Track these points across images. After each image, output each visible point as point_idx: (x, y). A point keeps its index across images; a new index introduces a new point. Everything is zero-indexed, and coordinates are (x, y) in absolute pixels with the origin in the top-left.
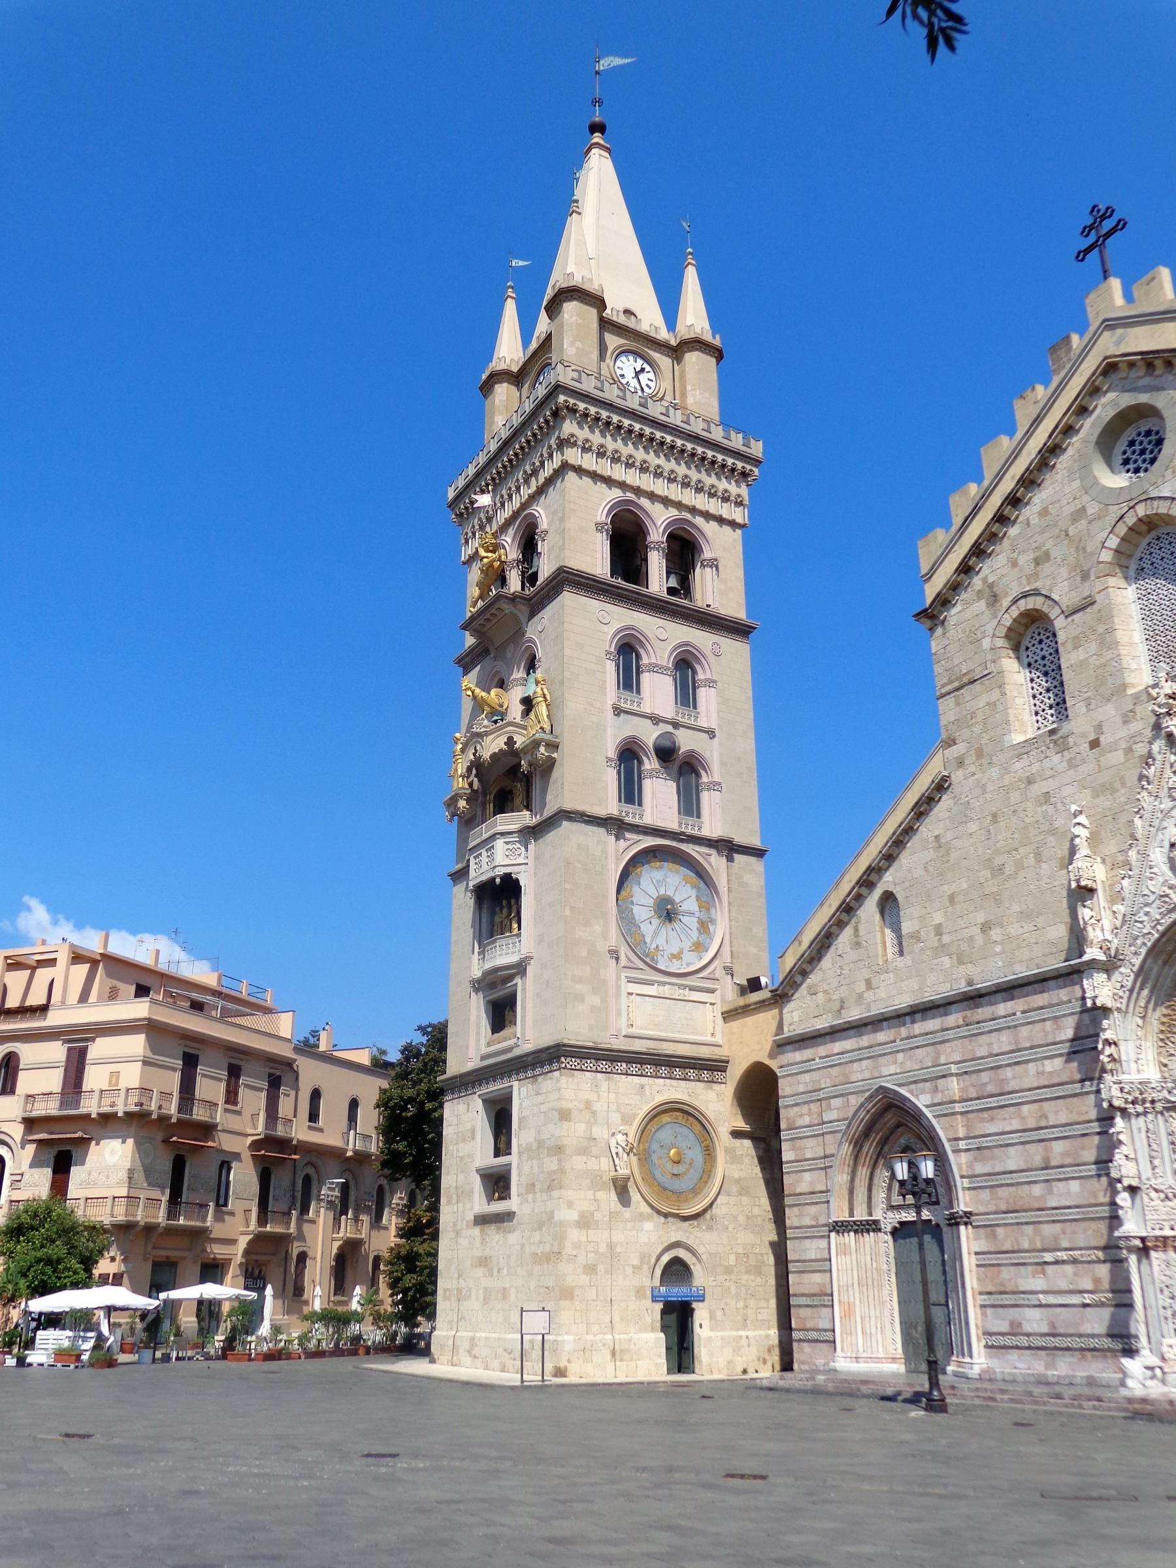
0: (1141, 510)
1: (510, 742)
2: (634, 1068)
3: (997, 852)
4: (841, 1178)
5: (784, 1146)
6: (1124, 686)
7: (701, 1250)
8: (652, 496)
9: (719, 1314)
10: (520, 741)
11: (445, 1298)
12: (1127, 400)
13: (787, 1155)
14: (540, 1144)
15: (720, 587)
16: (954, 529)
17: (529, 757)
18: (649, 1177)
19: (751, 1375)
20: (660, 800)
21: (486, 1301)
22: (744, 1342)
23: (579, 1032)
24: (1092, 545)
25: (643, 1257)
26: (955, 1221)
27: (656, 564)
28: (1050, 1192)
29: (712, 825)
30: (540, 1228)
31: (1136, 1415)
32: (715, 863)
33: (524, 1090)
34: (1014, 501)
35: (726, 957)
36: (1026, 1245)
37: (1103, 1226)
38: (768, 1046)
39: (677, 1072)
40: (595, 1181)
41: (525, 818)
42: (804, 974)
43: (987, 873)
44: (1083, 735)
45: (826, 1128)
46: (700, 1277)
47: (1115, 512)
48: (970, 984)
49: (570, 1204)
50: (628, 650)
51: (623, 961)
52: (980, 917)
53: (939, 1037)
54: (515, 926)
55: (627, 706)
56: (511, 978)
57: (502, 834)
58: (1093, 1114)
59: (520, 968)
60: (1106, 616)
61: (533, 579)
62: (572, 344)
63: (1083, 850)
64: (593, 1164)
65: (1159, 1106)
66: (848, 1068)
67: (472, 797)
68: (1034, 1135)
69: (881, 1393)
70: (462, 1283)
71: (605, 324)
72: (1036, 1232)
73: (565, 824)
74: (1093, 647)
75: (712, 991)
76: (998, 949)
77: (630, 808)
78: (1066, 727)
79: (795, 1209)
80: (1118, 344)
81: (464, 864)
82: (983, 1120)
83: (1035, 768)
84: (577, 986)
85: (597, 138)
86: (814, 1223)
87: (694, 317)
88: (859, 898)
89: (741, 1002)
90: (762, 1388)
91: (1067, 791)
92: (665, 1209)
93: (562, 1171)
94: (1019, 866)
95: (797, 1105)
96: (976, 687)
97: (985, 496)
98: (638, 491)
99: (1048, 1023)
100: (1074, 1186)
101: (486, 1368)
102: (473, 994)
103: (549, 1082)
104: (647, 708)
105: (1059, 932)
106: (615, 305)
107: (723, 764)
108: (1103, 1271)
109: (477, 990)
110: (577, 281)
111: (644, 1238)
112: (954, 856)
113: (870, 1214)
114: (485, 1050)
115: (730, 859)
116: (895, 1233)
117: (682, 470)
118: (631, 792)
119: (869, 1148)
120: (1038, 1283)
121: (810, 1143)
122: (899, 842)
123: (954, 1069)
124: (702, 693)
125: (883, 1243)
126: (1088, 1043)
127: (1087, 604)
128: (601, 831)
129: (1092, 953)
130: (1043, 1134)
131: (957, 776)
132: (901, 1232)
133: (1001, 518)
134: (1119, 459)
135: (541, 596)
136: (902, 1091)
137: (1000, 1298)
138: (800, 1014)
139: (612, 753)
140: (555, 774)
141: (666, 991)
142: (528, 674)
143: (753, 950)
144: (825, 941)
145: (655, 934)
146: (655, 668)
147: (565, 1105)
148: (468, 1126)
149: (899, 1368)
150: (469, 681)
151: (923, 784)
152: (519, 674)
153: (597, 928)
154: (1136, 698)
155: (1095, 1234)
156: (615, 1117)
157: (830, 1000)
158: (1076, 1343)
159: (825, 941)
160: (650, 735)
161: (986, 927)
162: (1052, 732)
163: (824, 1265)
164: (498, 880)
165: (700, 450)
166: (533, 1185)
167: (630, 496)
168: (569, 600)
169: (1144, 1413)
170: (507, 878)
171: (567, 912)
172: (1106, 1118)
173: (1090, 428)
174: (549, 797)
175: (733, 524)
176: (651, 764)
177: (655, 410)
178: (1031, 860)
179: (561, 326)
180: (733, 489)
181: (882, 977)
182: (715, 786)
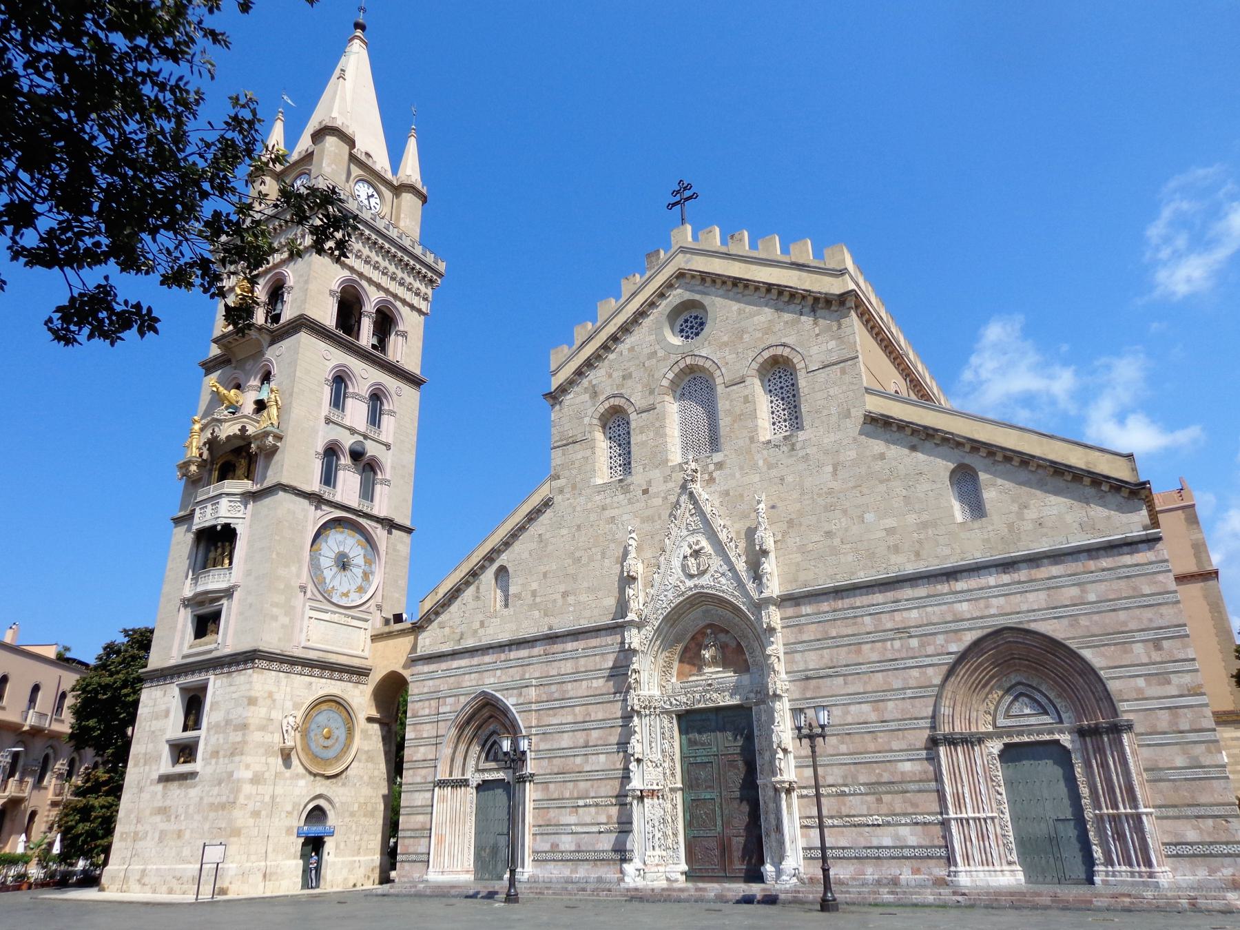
0: (688, 361)
1: (243, 429)
2: (307, 670)
4: (447, 751)
5: (408, 729)
6: (667, 460)
7: (336, 800)
8: (370, 281)
9: (342, 845)
10: (251, 430)
11: (122, 839)
12: (688, 296)
13: (410, 734)
14: (228, 722)
15: (406, 350)
16: (575, 347)
17: (258, 442)
18: (307, 748)
19: (359, 888)
20: (348, 487)
21: (161, 840)
22: (357, 864)
23: (270, 642)
24: (658, 375)
25: (295, 805)
26: (522, 780)
27: (367, 326)
28: (587, 761)
29: (380, 507)
30: (220, 784)
31: (632, 899)
32: (379, 533)
33: (219, 682)
34: (615, 338)
35: (378, 598)
36: (567, 795)
37: (617, 783)
38: (403, 661)
39: (336, 675)
40: (268, 752)
41: (248, 485)
42: (437, 614)
43: (570, 561)
44: (639, 485)
46: (332, 819)
47: (674, 358)
48: (550, 629)
49: (247, 767)
50: (340, 380)
51: (309, 595)
52: (562, 588)
53: (526, 661)
54: (227, 561)
55: (335, 418)
56: (221, 598)
57: (228, 494)
58: (619, 714)
59: (228, 593)
60: (662, 418)
61: (276, 318)
62: (329, 165)
63: (633, 554)
64: (268, 738)
65: (658, 711)
66: (461, 678)
67: (202, 464)
68: (581, 726)
69: (465, 892)
70: (140, 827)
71: (353, 158)
73: (281, 493)
74: (651, 435)
75: (366, 621)
76: (571, 609)
77: (326, 488)
78: (629, 479)
79: (411, 772)
80: (687, 262)
81: (188, 512)
82: (549, 715)
83: (608, 501)
84: (275, 610)
85: (359, 33)
87: (411, 170)
88: (483, 568)
89: (387, 629)
90: (377, 895)
91: (625, 517)
92: (315, 771)
93: (245, 742)
94: (591, 559)
96: (577, 446)
97: (597, 331)
98: (361, 275)
100: (602, 758)
101: (154, 892)
102: (182, 609)
104: (347, 422)
105: (611, 602)
106: (361, 147)
107: (393, 468)
108: (614, 811)
109: (186, 606)
110: (338, 123)
111: (297, 792)
112: (550, 548)
114: (186, 651)
115: (390, 533)
116: (478, 787)
117: (392, 268)
118: (329, 478)
119: (469, 731)
120: (572, 819)
121: (428, 727)
122: (514, 535)
123: (534, 682)
124: (385, 418)
125: (470, 794)
126: (622, 671)
127: (651, 408)
128: (306, 502)
129: (631, 616)
130: (586, 725)
131: (558, 499)
132: (483, 787)
133: (605, 347)
134: (678, 328)
135: (281, 332)
136: (498, 695)
137: (547, 829)
138: (428, 642)
139: (320, 449)
140: (277, 457)
141: (336, 618)
142: (262, 384)
143: (397, 595)
144: (454, 594)
145: (334, 577)
146: (356, 396)
147: (253, 694)
148: (163, 707)
149: (470, 877)
150: (212, 380)
151: (535, 500)
152: (255, 382)
153: (294, 569)
154: (673, 469)
155: (612, 788)
156: (289, 704)
158: (592, 856)
159: (454, 594)
160: (348, 441)
161: (565, 595)
162: (621, 481)
164: (219, 528)
165: (406, 258)
166: (217, 752)
167: (355, 277)
168: (304, 337)
169: (637, 897)
170: (227, 527)
171: (274, 556)
172: (627, 717)
173: (665, 306)
174: (270, 473)
175: (420, 311)
176: (345, 460)
177: (380, 224)
179: (323, 151)
180: (423, 289)
182: (386, 482)
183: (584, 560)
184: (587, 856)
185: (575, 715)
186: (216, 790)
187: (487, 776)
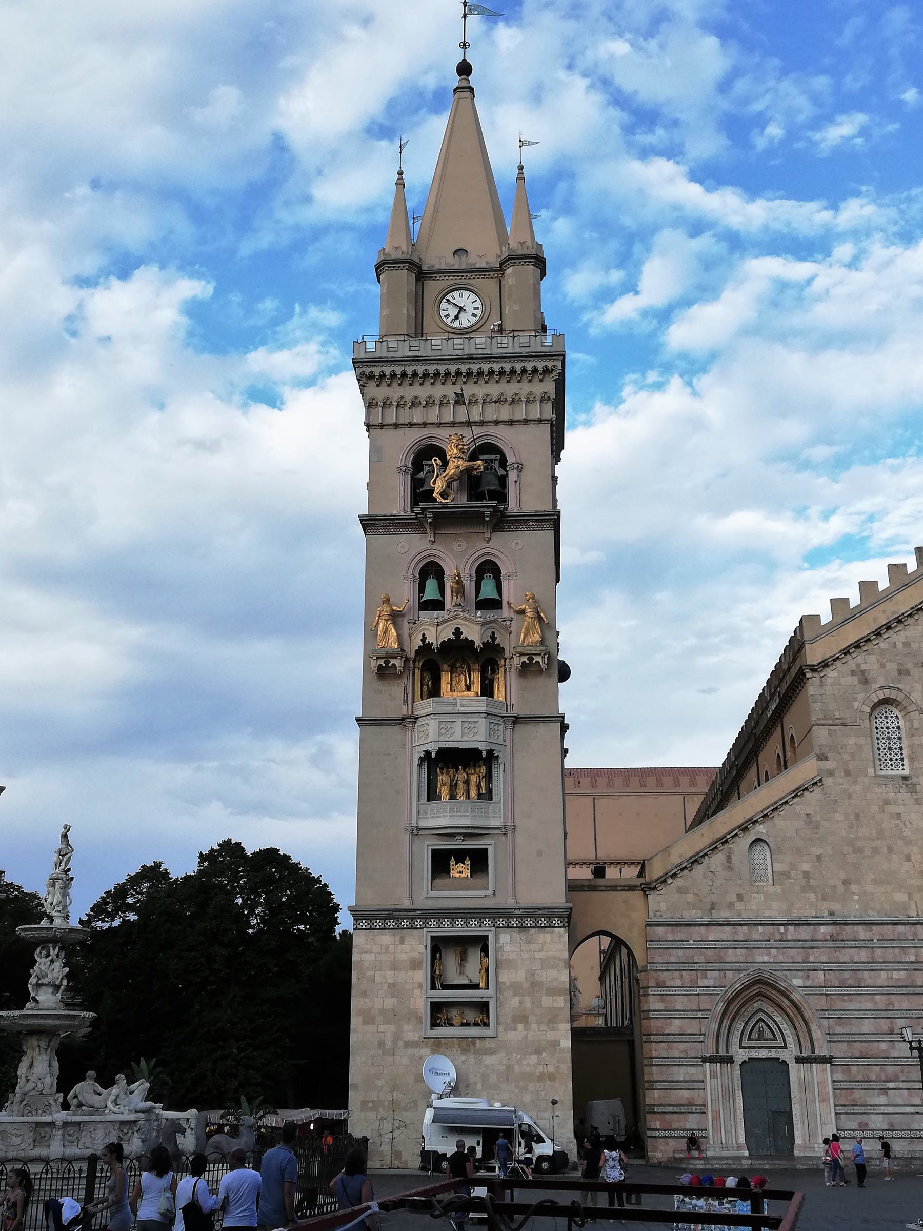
3: (858, 838)
14: (534, 984)
28: (894, 1047)
33: (505, 937)
36: (874, 1078)
45: (698, 991)
52: (843, 875)
66: (722, 952)
72: (881, 1070)
82: (844, 1000)
83: (891, 795)
86: (682, 1055)
94: (875, 850)
95: (667, 970)
99: (897, 950)
103: (548, 937)
113: (727, 1052)
130: (889, 1014)
131: (828, 781)
157: (700, 901)
163: (696, 1084)
178: (885, 850)
181: (753, 895)
183: (867, 852)
184: (903, 1134)
185: (876, 1003)
186: (534, 1059)
187: (755, 1054)
